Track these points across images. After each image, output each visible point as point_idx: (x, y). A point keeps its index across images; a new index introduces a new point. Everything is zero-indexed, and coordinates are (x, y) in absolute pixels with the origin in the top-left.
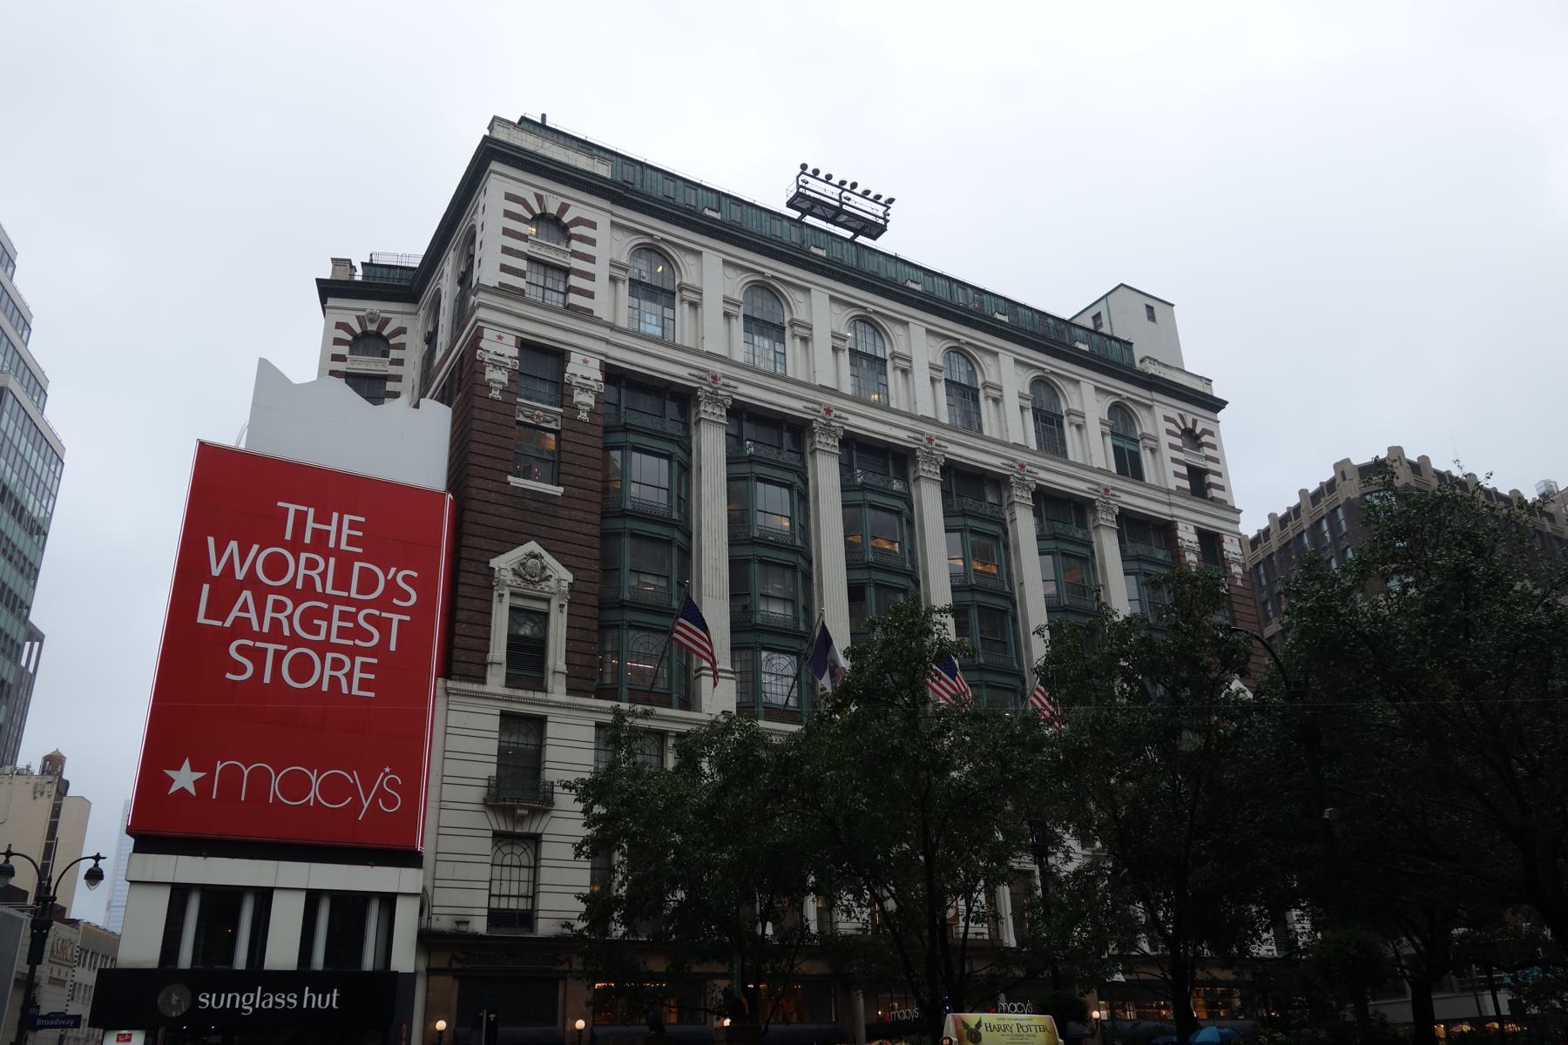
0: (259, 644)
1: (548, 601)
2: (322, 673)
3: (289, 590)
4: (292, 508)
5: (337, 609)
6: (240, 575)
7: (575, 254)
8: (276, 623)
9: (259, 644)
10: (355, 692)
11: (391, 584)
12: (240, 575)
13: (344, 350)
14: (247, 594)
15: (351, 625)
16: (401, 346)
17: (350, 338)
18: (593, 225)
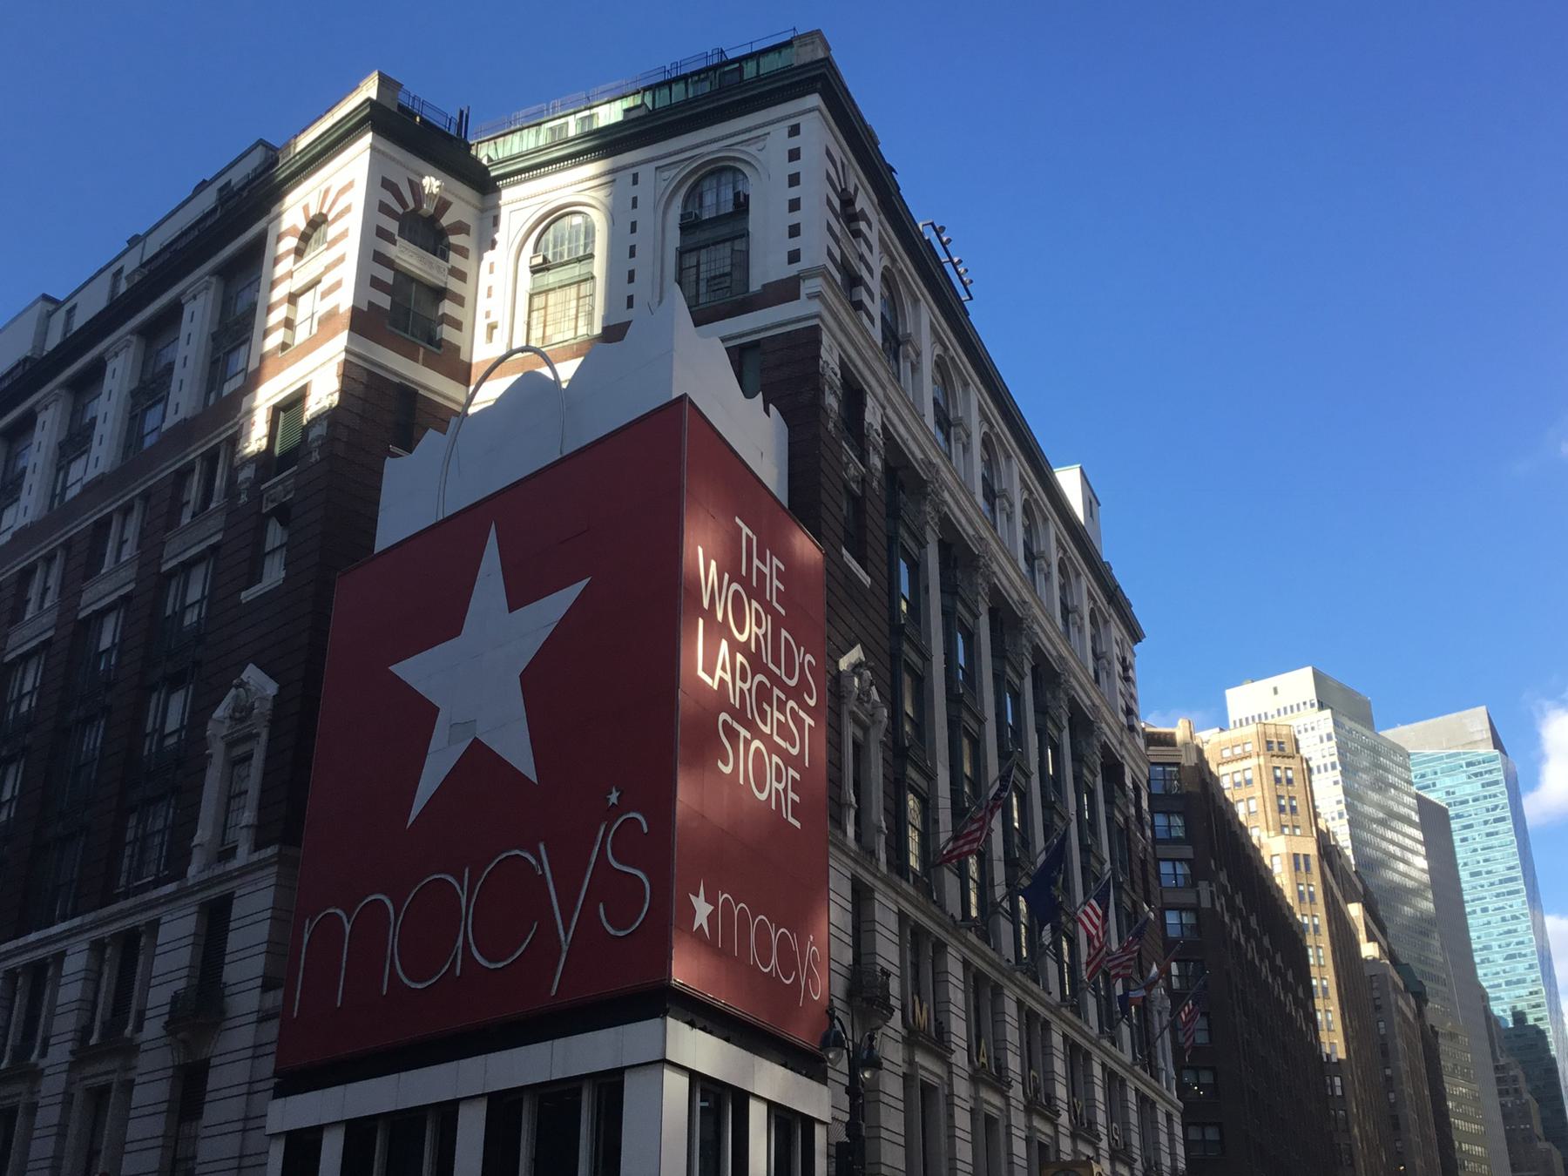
0: (736, 725)
1: (866, 729)
2: (773, 785)
3: (744, 648)
4: (746, 530)
5: (776, 691)
6: (720, 617)
7: (861, 257)
8: (742, 690)
9: (736, 725)
10: (791, 819)
11: (801, 665)
12: (720, 617)
13: (392, 226)
14: (724, 645)
15: (782, 718)
16: (463, 252)
17: (400, 210)
18: (870, 225)
